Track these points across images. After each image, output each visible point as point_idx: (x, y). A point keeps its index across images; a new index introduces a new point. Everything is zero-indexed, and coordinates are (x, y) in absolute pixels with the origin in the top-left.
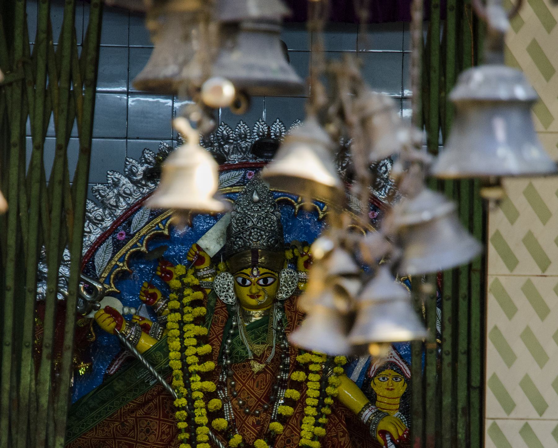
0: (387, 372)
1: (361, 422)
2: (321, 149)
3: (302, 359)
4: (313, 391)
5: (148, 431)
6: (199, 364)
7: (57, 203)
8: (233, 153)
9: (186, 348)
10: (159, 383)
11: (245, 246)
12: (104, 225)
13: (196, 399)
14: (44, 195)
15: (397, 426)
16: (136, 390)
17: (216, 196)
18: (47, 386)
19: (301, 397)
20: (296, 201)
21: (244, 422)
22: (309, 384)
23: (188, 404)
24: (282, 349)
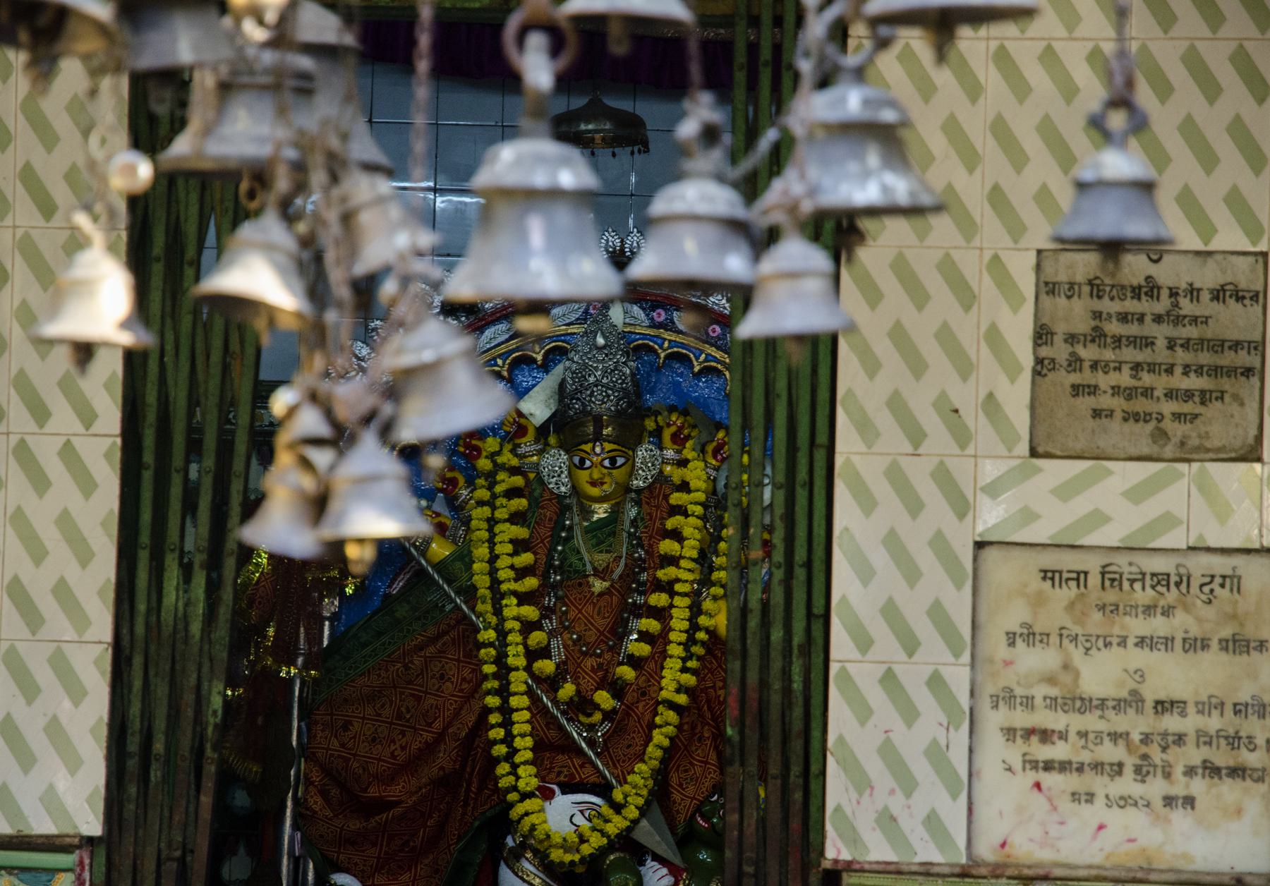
2: (282, 259)
4: (679, 620)
5: (442, 677)
6: (516, 580)
7: (217, 343)
9: (497, 557)
10: (458, 608)
11: (584, 412)
13: (510, 631)
14: (200, 331)
17: (125, 325)
18: (200, 608)
19: (663, 630)
20: (661, 347)
21: (579, 666)
22: (674, 611)
23: (498, 639)
24: (635, 560)
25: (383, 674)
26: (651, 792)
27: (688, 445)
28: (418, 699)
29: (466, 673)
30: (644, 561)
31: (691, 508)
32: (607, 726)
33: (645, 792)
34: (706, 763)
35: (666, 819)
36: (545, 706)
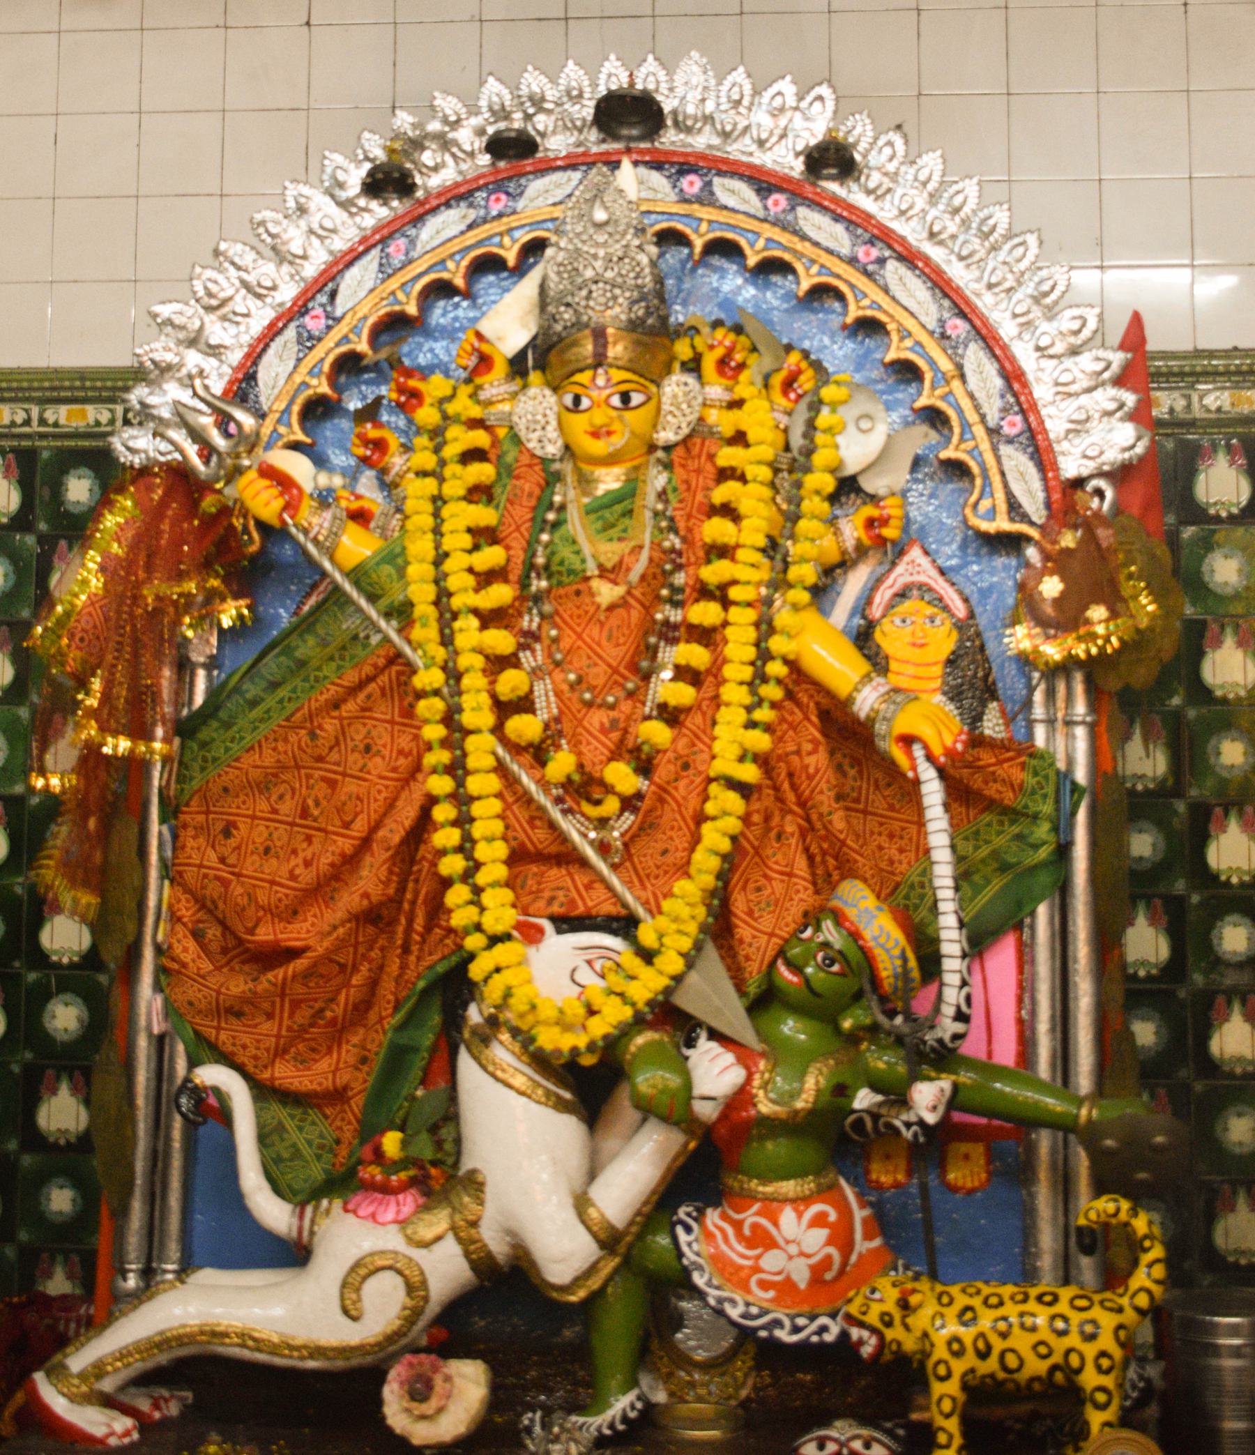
0: (907, 605)
1: (855, 720)
3: (714, 573)
4: (739, 645)
5: (368, 749)
6: (477, 590)
8: (554, 132)
9: (447, 555)
10: (387, 640)
12: (279, 299)
15: (942, 728)
16: (342, 658)
21: (580, 722)
24: (665, 552)
25: (281, 746)
26: (703, 928)
27: (744, 376)
28: (332, 784)
29: (404, 742)
30: (680, 554)
31: (751, 471)
32: (628, 819)
33: (692, 928)
34: (790, 875)
35: (729, 969)
36: (526, 793)
